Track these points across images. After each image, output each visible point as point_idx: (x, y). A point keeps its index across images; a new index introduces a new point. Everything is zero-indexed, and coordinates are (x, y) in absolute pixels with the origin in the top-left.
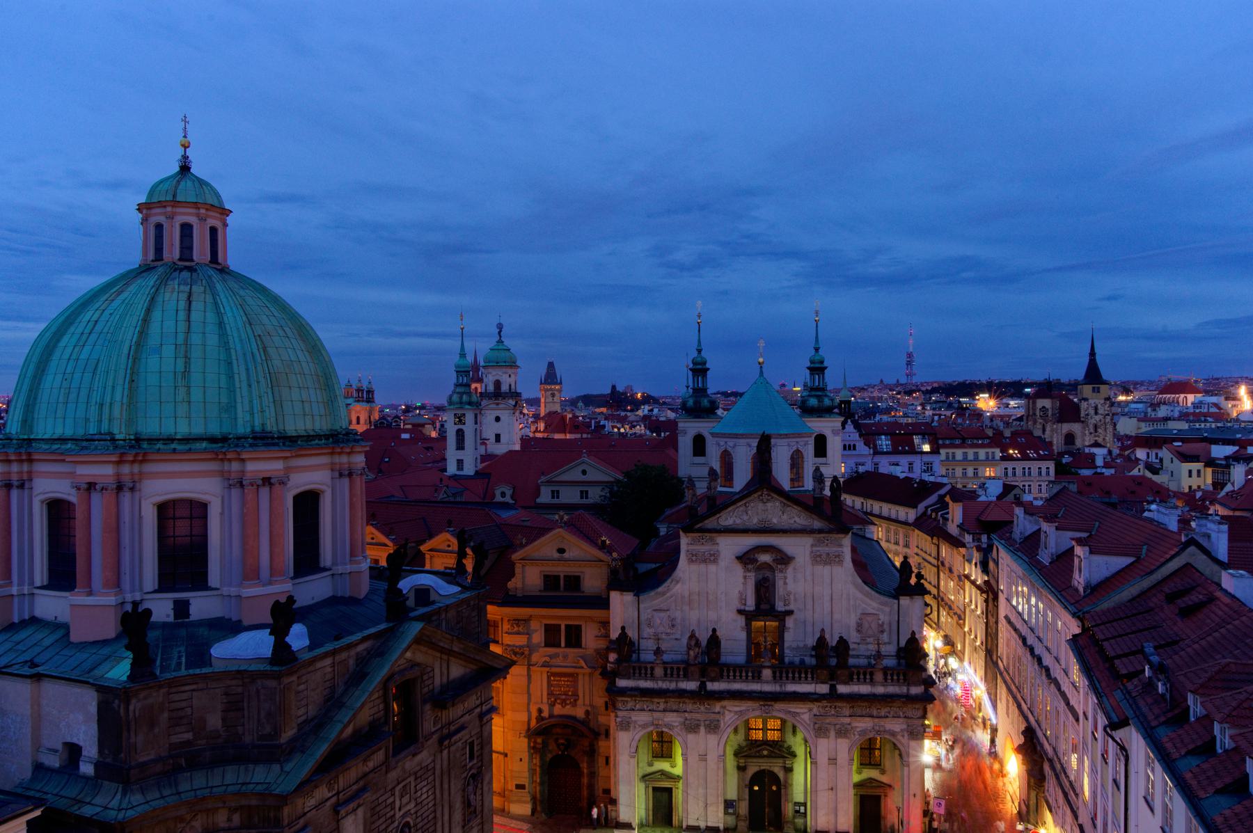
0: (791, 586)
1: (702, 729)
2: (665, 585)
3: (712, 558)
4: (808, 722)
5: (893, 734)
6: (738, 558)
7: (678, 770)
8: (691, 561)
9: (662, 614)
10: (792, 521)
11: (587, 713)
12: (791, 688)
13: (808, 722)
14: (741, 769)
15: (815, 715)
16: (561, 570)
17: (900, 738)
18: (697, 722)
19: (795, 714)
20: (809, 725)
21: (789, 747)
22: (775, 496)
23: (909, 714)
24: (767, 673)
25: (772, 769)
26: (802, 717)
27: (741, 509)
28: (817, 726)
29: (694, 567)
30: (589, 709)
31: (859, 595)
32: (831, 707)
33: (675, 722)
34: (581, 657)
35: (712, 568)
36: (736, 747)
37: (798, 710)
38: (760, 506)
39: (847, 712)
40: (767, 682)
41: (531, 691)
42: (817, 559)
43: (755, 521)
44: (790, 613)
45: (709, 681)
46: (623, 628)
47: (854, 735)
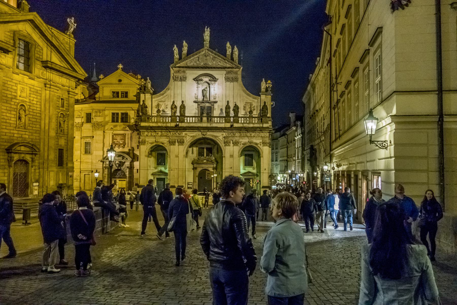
1: (177, 144)
2: (164, 90)
5: (256, 144)
6: (194, 79)
7: (167, 171)
8: (175, 80)
11: (129, 150)
12: (214, 125)
13: (222, 140)
14: (194, 169)
17: (259, 145)
19: (216, 137)
20: (222, 141)
22: (211, 53)
23: (263, 135)
24: (205, 119)
25: (208, 168)
27: (196, 59)
28: (225, 141)
30: (130, 148)
31: (246, 95)
33: (165, 141)
34: (127, 126)
36: (193, 159)
37: (217, 135)
38: (205, 58)
39: (237, 134)
40: (205, 123)
41: (104, 142)
42: (227, 79)
43: (202, 64)
44: (216, 102)
46: (143, 101)
47: (241, 144)
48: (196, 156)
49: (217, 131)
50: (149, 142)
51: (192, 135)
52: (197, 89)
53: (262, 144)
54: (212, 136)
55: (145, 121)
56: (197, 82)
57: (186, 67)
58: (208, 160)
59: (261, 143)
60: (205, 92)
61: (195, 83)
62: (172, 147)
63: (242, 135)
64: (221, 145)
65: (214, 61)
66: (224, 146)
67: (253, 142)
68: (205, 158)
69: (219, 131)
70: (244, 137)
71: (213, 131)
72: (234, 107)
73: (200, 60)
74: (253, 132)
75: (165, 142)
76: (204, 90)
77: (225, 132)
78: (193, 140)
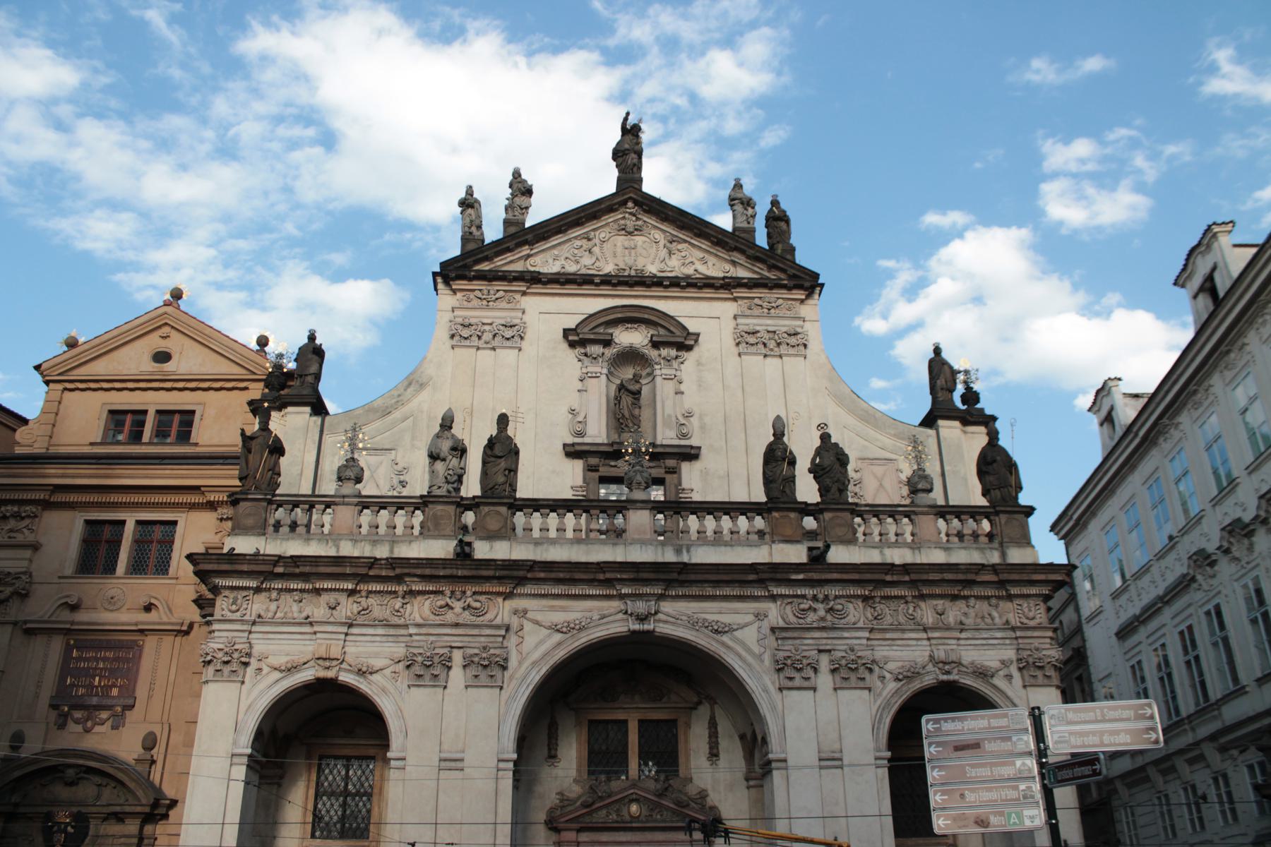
0: (691, 400)
1: (457, 675)
3: (508, 333)
4: (756, 649)
9: (373, 460)
10: (689, 271)
13: (756, 649)
15: (773, 630)
16: (153, 401)
17: (999, 681)
18: (441, 651)
20: (759, 657)
21: (703, 795)
22: (652, 221)
26: (736, 633)
27: (578, 243)
28: (781, 655)
29: (465, 354)
30: (157, 729)
32: (815, 598)
33: (377, 655)
35: (507, 356)
37: (726, 619)
38: (621, 240)
39: (855, 613)
40: (643, 542)
42: (746, 340)
43: (609, 268)
44: (691, 455)
45: (481, 539)
47: (882, 678)
48: (573, 773)
49: (728, 591)
50: (274, 661)
51: (559, 618)
52: (579, 385)
53: (1016, 674)
54: (693, 624)
55: (260, 529)
56: (580, 350)
57: (521, 277)
58: (655, 807)
59: (1014, 670)
60: (627, 400)
61: (569, 360)
62: (421, 696)
63: (888, 619)
64: (751, 683)
65: (670, 253)
66: (773, 690)
67: (960, 664)
68: (634, 786)
69: (737, 592)
70: (899, 628)
71: (695, 590)
72: (818, 452)
73: (596, 250)
74: (954, 598)
75: (377, 663)
76: (621, 387)
77: (773, 598)
78: (561, 654)
